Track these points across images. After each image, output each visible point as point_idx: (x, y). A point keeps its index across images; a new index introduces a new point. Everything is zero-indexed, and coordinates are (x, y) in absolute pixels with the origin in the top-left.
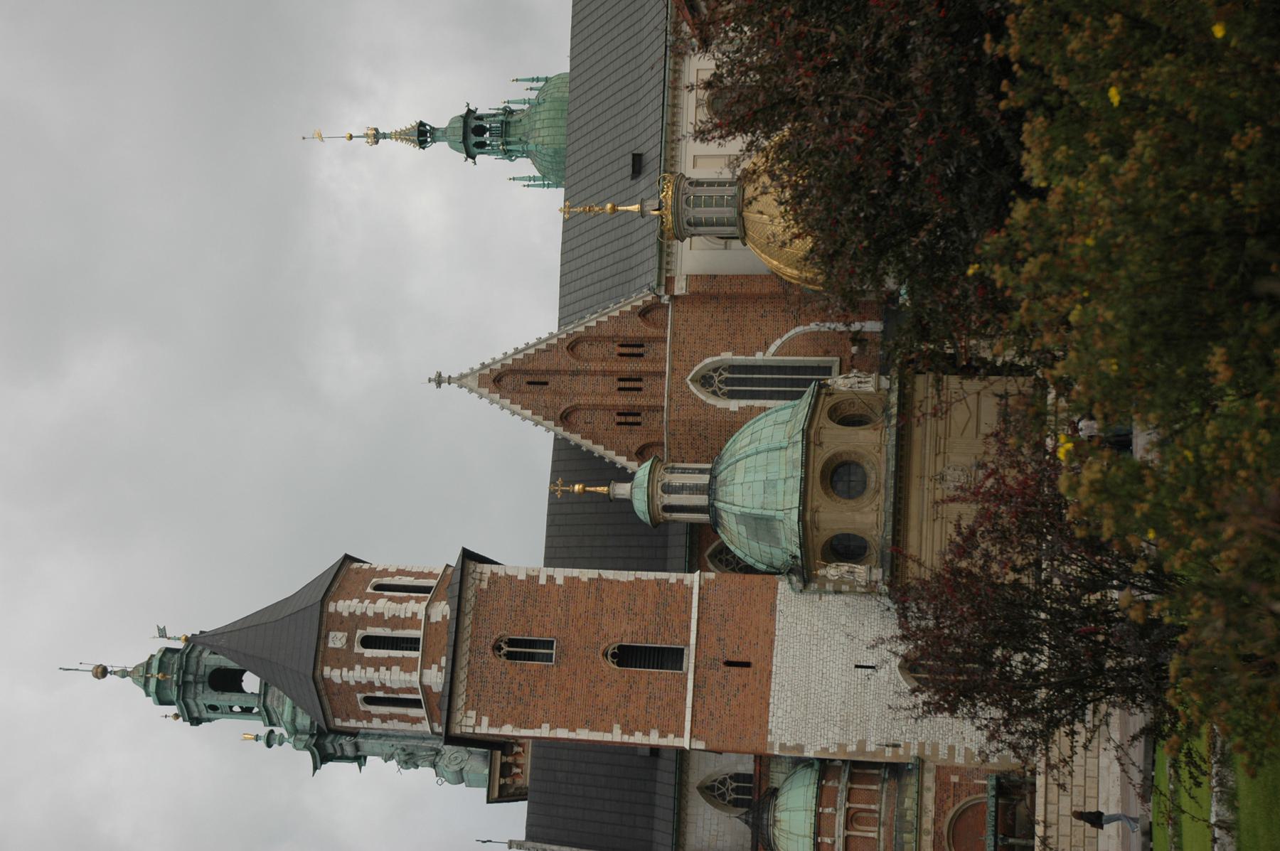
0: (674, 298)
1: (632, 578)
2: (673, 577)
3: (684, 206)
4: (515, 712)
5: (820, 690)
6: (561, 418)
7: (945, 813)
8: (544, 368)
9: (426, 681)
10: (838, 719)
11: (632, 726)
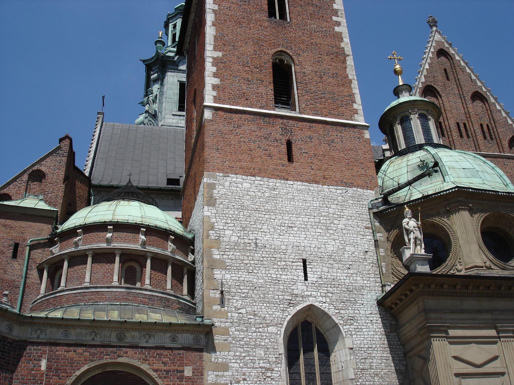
1: (350, 77)
5: (275, 224)
6: (429, 85)
7: (145, 360)
8: (460, 77)
10: (246, 241)
11: (222, 65)
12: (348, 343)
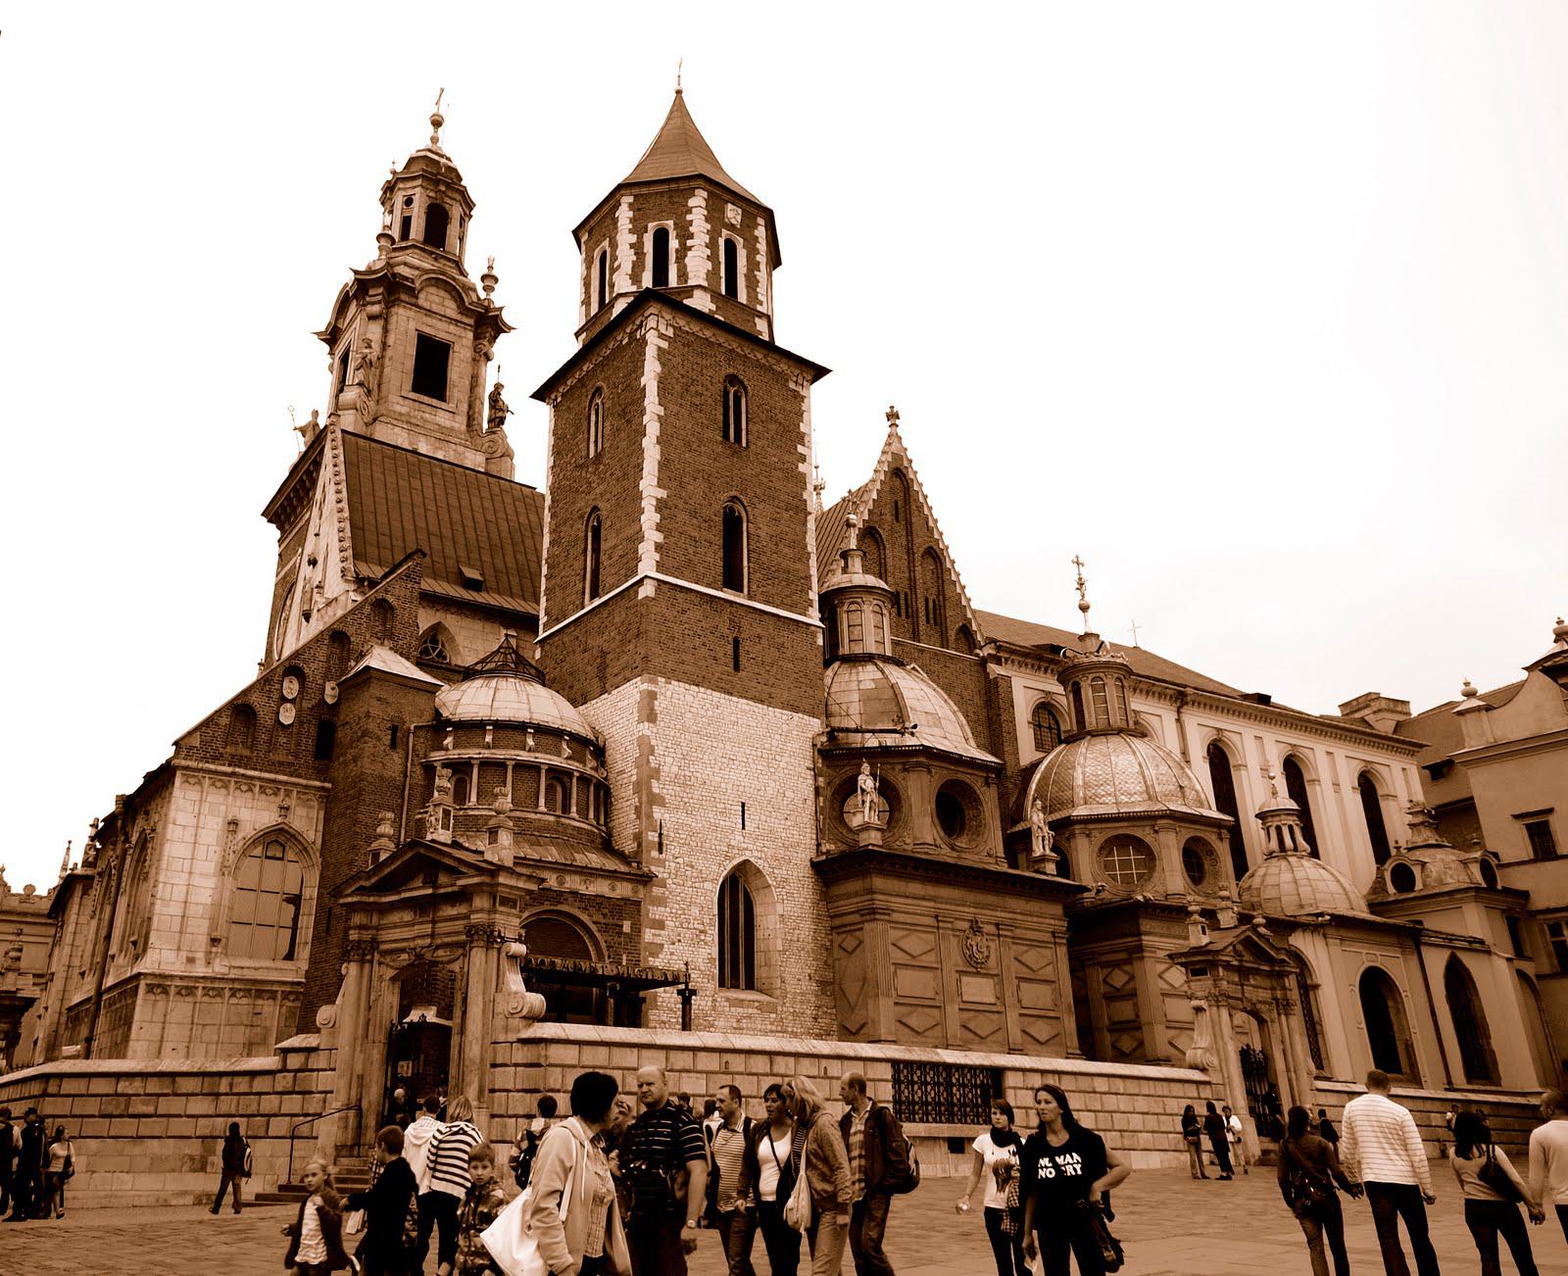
0: (983, 662)
1: (810, 549)
2: (814, 596)
3: (1091, 676)
4: (674, 381)
9: (697, 293)
10: (687, 773)
12: (779, 909)
